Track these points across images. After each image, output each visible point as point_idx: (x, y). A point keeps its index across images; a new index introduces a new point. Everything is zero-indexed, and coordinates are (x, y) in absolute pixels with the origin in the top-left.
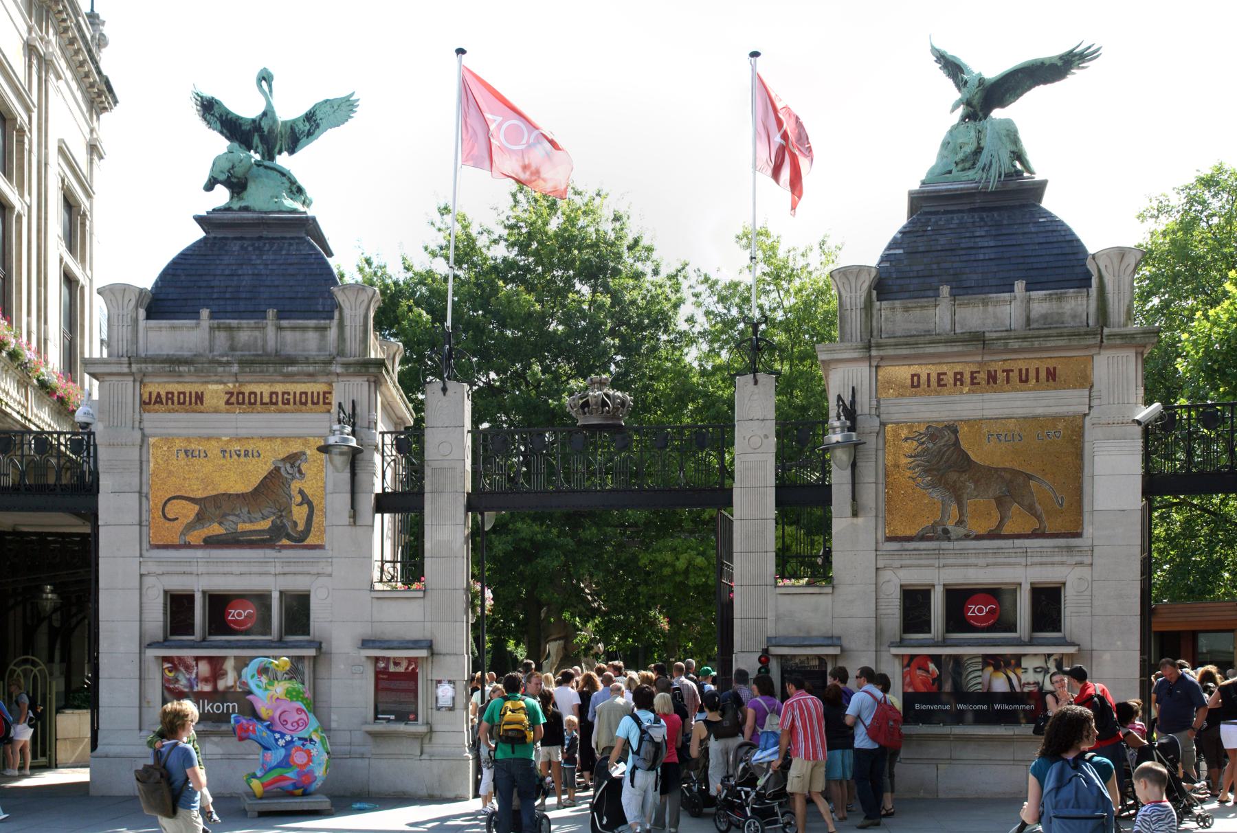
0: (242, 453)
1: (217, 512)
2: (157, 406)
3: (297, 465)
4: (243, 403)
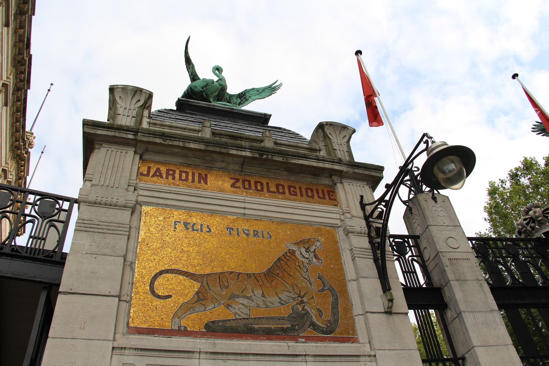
0: (252, 233)
1: (224, 293)
2: (155, 179)
3: (312, 249)
4: (250, 188)
